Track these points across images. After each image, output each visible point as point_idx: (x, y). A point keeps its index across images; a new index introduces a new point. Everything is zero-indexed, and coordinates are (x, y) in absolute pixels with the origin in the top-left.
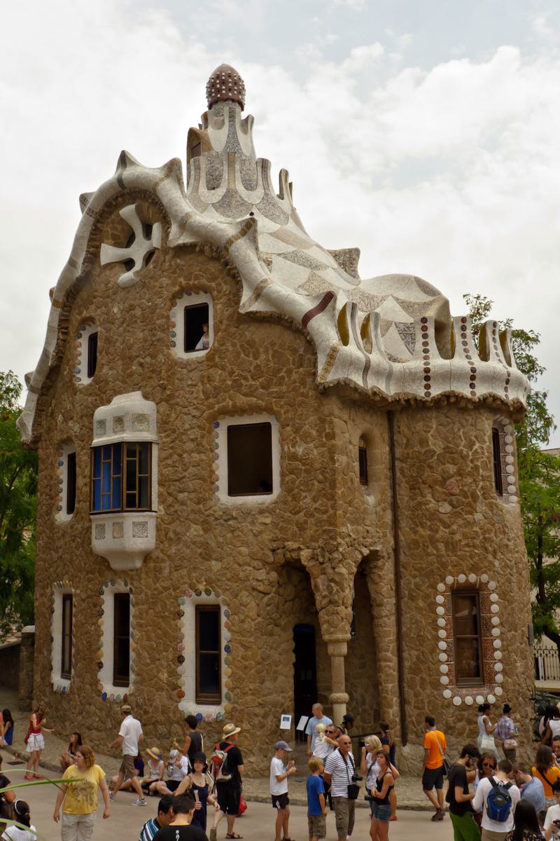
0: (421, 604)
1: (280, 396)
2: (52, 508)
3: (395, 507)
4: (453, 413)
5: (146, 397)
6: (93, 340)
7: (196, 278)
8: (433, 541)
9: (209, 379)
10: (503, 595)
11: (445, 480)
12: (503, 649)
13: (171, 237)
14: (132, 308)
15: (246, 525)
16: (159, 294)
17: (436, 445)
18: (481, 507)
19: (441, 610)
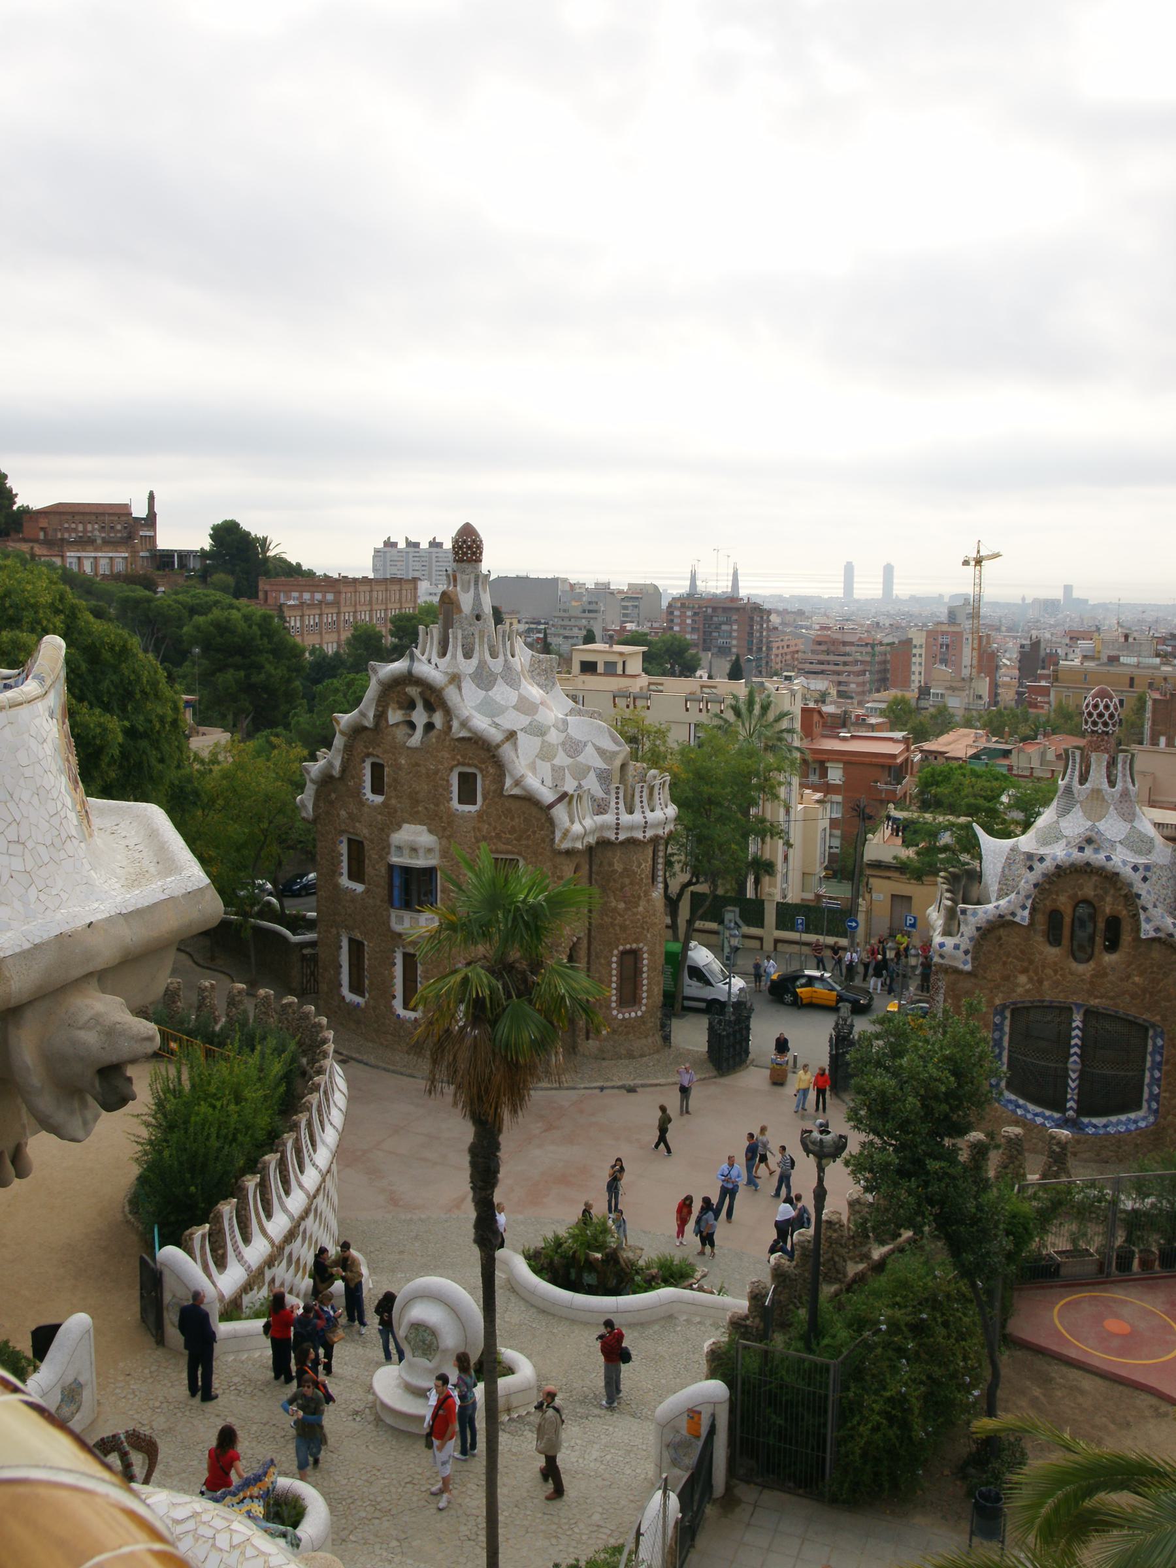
0: (603, 961)
1: (527, 847)
2: (335, 872)
5: (430, 831)
6: (377, 769)
7: (470, 758)
9: (479, 830)
10: (651, 953)
11: (622, 888)
12: (649, 983)
13: (454, 730)
14: (417, 765)
16: (442, 763)
17: (618, 867)
18: (642, 903)
19: (614, 966)
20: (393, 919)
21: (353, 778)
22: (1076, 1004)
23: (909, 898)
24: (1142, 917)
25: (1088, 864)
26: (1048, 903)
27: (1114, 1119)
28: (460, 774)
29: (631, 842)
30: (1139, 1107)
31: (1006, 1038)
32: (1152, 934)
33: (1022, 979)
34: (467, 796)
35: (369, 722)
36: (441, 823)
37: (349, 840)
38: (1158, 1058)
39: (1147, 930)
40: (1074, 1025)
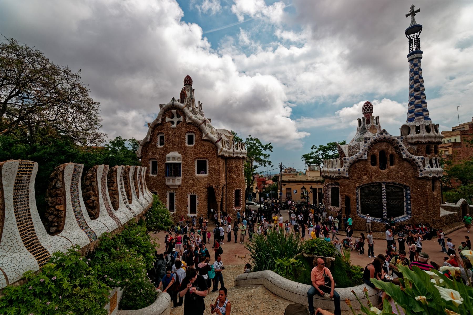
1: (209, 156)
3: (226, 176)
4: (237, 159)
5: (179, 153)
6: (162, 138)
8: (233, 182)
9: (194, 151)
14: (175, 133)
15: (202, 180)
17: (234, 165)
18: (240, 176)
20: (167, 181)
21: (154, 141)
22: (383, 182)
23: (290, 189)
24: (402, 152)
25: (385, 138)
26: (371, 153)
27: (397, 218)
28: (188, 135)
29: (238, 158)
30: (403, 214)
31: (359, 197)
32: (406, 157)
33: (365, 177)
34: (190, 142)
35: (160, 121)
36: (183, 150)
37: (152, 162)
38: (409, 197)
39: (404, 156)
40: (383, 189)
